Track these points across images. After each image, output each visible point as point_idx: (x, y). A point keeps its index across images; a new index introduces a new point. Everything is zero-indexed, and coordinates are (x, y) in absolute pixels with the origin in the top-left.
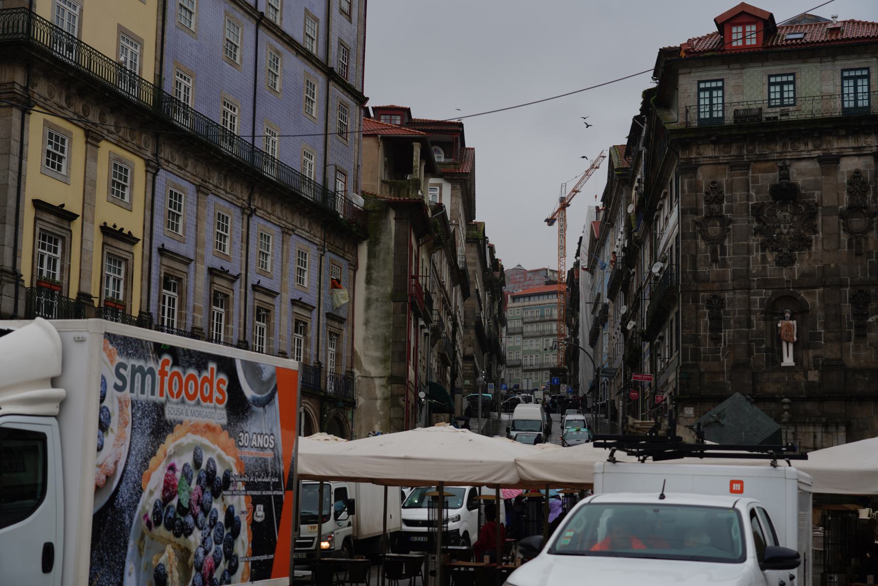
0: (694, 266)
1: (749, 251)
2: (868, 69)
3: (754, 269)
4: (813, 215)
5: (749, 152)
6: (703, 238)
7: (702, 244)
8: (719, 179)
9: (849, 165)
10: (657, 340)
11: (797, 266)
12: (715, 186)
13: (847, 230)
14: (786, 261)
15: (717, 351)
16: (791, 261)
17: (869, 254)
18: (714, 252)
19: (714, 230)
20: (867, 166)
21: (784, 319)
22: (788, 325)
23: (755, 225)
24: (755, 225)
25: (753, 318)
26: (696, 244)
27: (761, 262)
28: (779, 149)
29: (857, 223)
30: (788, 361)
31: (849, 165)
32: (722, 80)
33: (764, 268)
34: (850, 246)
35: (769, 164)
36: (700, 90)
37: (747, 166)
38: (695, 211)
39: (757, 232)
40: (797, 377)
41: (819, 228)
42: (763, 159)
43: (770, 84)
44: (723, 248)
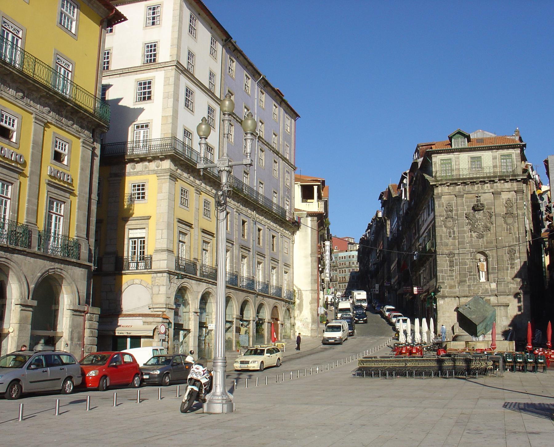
0: (441, 239)
1: (464, 232)
3: (467, 240)
4: (491, 217)
5: (464, 190)
9: (505, 196)
10: (422, 271)
11: (485, 239)
12: (449, 205)
13: (505, 222)
14: (480, 236)
15: (452, 276)
16: (483, 237)
17: (515, 233)
18: (450, 233)
19: (449, 224)
20: (512, 196)
24: (467, 221)
25: (467, 261)
26: (442, 230)
27: (469, 237)
28: (476, 189)
29: (510, 221)
31: (505, 196)
34: (507, 230)
36: (442, 164)
38: (443, 216)
40: (486, 286)
44: (454, 232)
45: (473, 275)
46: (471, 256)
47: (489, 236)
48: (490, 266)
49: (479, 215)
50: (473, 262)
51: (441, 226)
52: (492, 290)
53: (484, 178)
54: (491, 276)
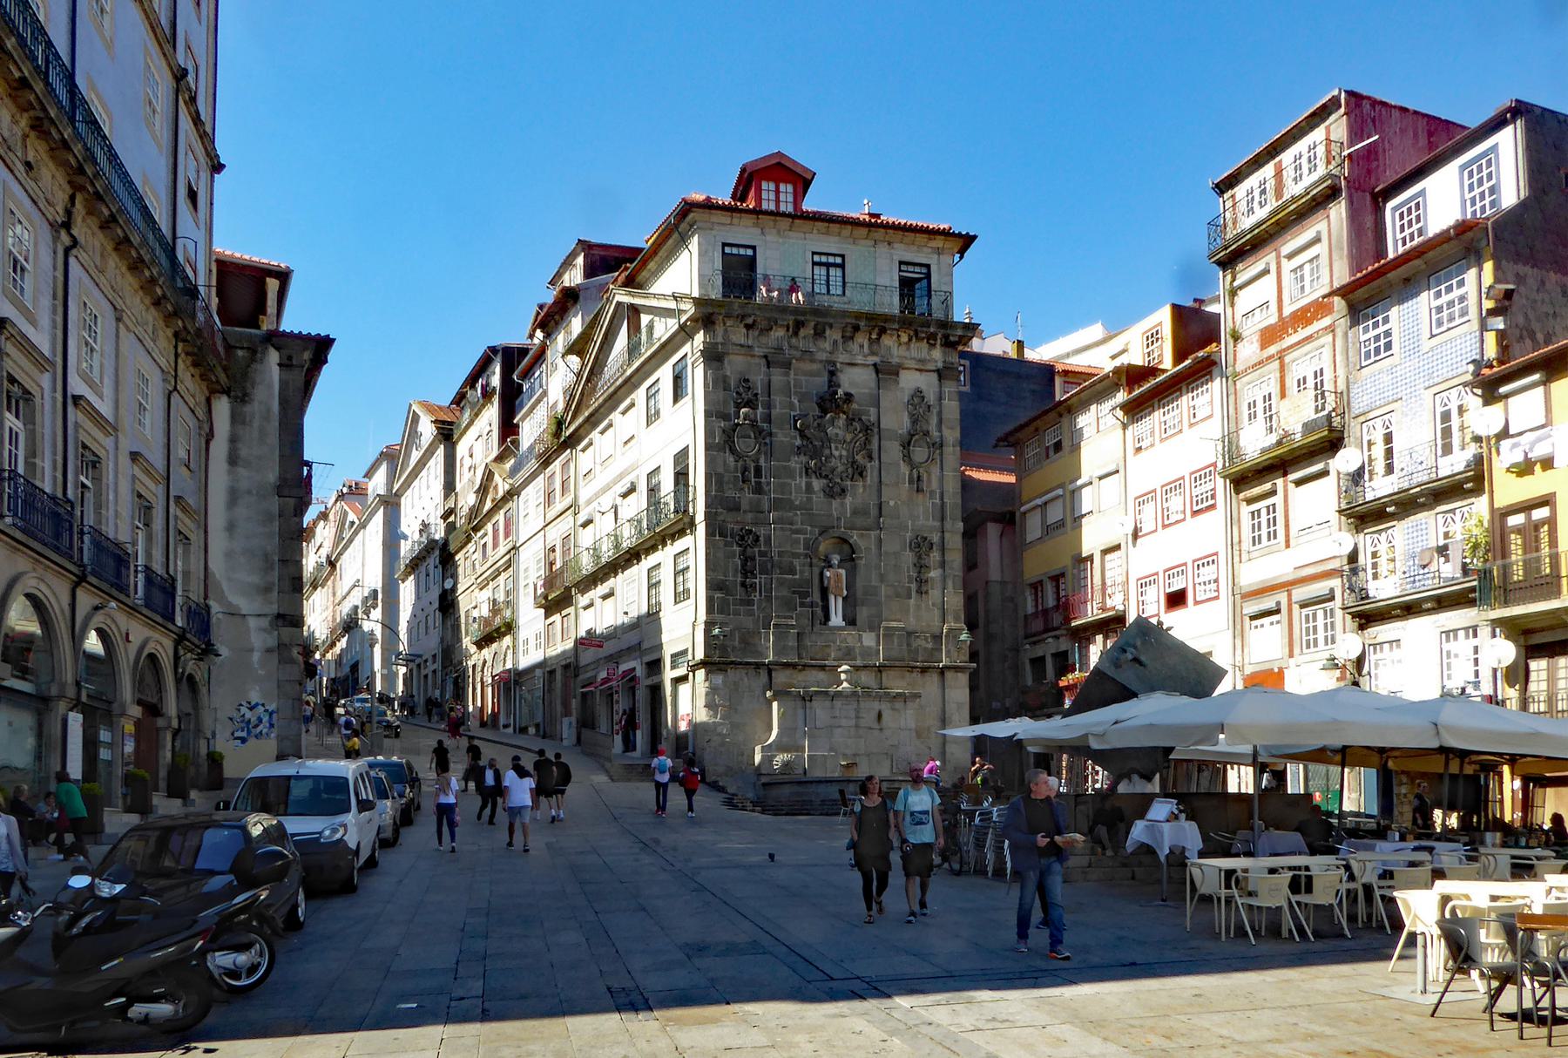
1: (790, 473)
2: (928, 266)
6: (733, 451)
7: (731, 459)
8: (752, 378)
11: (848, 500)
13: (907, 457)
15: (750, 603)
17: (932, 492)
18: (745, 469)
21: (830, 566)
22: (836, 575)
23: (798, 442)
24: (798, 442)
25: (796, 562)
28: (827, 345)
30: (836, 619)
31: (910, 380)
32: (754, 248)
33: (809, 500)
35: (815, 366)
37: (787, 365)
38: (726, 417)
39: (799, 450)
41: (875, 455)
42: (807, 355)
43: (814, 264)
44: (758, 471)
45: (812, 605)
46: (807, 547)
47: (859, 493)
48: (860, 583)
49: (837, 428)
50: (811, 565)
51: (721, 448)
52: (867, 652)
53: (859, 316)
54: (863, 614)
